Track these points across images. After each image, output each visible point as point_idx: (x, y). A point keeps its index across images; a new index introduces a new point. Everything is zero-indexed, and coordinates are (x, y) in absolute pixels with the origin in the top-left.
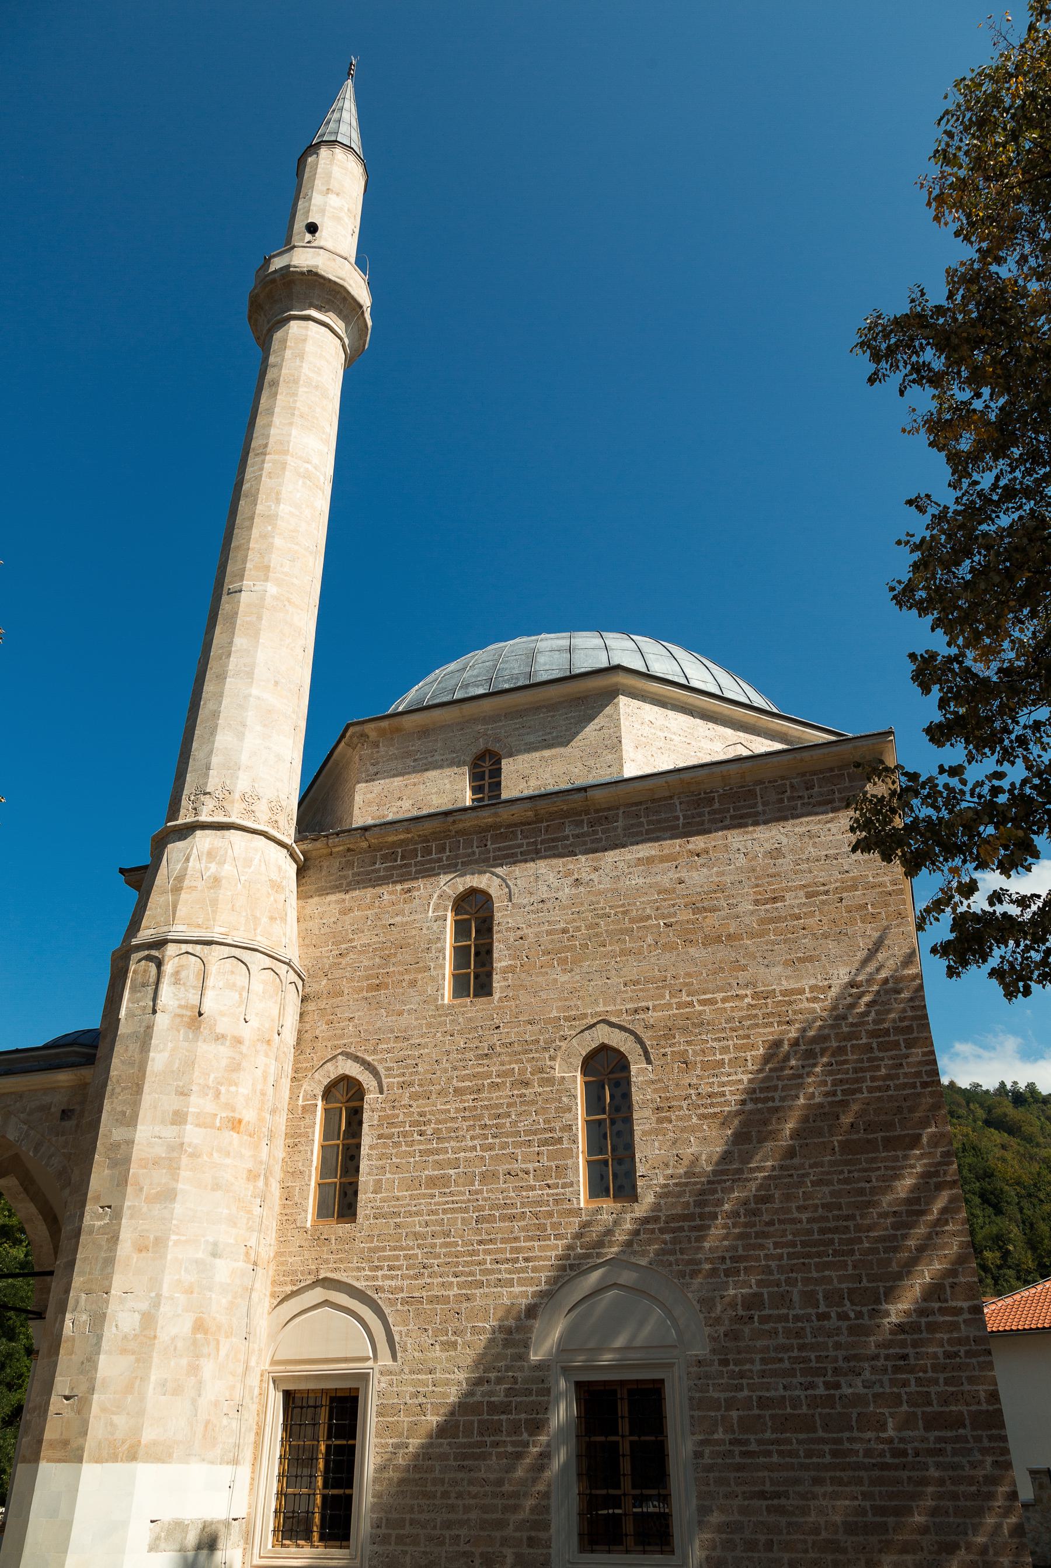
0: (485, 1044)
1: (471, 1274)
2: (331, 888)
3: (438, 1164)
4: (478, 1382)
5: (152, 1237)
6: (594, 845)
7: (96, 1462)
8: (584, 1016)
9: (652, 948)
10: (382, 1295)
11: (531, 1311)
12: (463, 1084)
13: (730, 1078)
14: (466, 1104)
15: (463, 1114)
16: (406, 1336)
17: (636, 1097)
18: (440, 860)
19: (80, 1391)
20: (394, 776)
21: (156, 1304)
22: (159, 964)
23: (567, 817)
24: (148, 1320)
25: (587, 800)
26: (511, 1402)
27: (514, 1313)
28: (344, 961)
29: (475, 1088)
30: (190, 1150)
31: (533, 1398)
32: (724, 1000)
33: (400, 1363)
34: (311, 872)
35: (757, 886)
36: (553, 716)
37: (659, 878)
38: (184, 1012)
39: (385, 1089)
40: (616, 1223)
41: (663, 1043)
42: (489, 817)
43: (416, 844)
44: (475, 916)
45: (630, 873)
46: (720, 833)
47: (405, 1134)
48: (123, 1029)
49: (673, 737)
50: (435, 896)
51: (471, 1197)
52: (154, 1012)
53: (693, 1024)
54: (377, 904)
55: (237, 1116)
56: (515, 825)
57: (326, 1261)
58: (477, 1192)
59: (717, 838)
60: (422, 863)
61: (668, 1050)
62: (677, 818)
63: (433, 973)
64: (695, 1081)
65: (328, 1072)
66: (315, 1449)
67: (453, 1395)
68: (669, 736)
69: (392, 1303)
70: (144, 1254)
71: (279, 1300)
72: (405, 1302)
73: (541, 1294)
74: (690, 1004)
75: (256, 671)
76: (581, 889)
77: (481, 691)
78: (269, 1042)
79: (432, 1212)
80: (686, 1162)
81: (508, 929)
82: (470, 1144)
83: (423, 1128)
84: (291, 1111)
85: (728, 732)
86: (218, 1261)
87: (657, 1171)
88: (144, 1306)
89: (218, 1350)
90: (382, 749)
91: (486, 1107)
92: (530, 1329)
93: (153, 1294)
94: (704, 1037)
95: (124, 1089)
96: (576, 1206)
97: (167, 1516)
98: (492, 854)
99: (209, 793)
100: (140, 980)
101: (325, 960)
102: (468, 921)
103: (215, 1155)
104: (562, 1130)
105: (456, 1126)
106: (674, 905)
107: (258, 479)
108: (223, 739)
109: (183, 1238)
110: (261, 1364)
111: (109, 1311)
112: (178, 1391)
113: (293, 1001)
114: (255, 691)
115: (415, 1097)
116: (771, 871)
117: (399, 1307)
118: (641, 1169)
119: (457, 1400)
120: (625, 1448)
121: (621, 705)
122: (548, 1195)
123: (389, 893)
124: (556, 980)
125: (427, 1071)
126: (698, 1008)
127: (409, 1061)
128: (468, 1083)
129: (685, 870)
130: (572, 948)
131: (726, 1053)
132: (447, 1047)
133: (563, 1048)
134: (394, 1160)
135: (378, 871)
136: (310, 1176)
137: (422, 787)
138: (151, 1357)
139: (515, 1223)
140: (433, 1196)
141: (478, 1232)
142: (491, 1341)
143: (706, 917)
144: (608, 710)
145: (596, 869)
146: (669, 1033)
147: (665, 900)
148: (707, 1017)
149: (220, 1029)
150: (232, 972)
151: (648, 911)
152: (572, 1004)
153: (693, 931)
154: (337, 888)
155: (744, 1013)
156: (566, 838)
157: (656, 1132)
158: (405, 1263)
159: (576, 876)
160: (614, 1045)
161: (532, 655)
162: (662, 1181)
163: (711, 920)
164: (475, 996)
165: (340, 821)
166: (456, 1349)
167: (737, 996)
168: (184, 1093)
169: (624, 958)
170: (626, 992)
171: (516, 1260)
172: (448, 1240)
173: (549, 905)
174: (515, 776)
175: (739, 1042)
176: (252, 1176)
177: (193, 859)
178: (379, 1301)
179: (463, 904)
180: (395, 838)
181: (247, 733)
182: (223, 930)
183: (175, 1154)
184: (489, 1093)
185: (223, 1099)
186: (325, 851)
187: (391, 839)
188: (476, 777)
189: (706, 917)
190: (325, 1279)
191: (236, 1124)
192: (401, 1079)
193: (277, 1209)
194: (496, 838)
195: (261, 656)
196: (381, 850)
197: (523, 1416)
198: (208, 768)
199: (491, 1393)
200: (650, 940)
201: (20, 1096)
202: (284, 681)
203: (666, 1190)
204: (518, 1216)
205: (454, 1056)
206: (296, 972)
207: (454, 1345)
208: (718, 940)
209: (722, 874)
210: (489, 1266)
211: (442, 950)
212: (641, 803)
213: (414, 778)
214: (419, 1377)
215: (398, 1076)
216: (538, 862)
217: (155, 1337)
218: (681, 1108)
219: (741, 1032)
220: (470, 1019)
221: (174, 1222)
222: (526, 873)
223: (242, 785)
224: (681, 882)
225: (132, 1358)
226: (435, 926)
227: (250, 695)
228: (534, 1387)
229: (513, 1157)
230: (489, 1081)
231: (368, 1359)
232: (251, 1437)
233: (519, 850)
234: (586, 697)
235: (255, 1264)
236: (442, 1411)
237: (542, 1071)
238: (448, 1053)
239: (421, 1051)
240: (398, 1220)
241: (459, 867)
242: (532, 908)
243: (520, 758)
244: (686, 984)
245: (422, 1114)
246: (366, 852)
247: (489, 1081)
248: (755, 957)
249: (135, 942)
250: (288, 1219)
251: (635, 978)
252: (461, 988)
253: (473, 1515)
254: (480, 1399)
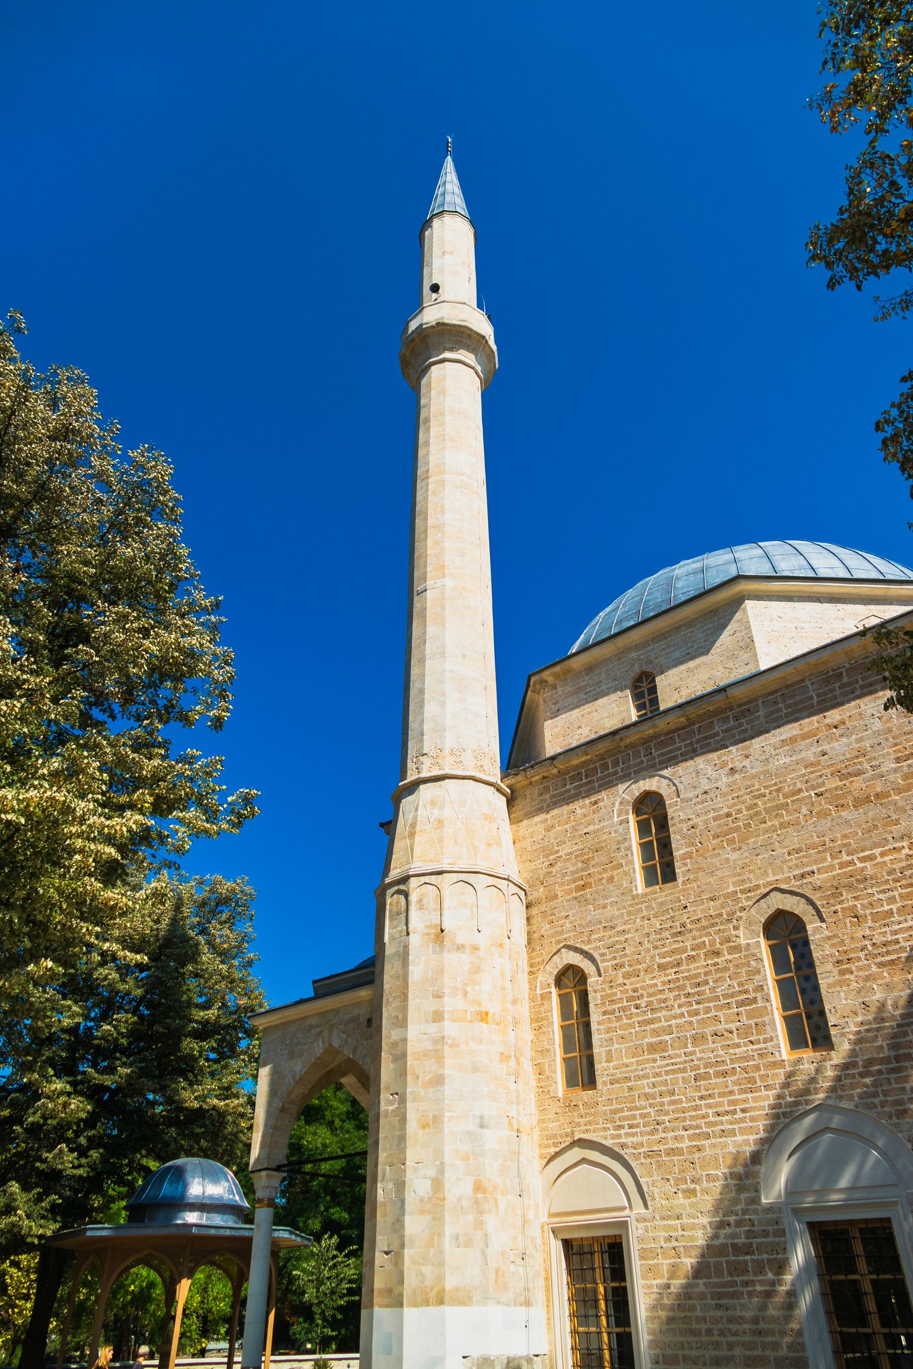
0: (677, 924)
1: (698, 1127)
2: (535, 811)
3: (655, 1032)
4: (721, 1225)
5: (431, 1116)
6: (742, 736)
7: (414, 1306)
8: (758, 887)
9: (808, 817)
10: (627, 1151)
11: (756, 1158)
12: (665, 960)
13: (901, 926)
14: (670, 978)
15: (668, 987)
16: (653, 1186)
17: (816, 954)
18: (616, 773)
19: (395, 1247)
20: (573, 709)
21: (442, 1171)
22: (406, 895)
23: (715, 716)
24: (437, 1184)
25: (728, 698)
26: (751, 1243)
27: (741, 1160)
28: (554, 870)
29: (675, 962)
30: (450, 1041)
31: (771, 1239)
32: (883, 854)
33: (651, 1210)
34: (518, 801)
35: (896, 745)
36: (692, 631)
37: (803, 755)
38: (430, 931)
39: (602, 972)
40: (818, 1071)
41: (832, 901)
42: (649, 729)
43: (596, 762)
44: (652, 812)
45: (777, 754)
46: (853, 703)
47: (624, 1009)
48: (388, 951)
49: (803, 625)
50: (617, 803)
51: (687, 1059)
52: (408, 934)
53: (857, 880)
54: (572, 818)
55: (484, 1009)
56: (672, 731)
57: (579, 1125)
58: (691, 1054)
59: (850, 708)
60: (602, 778)
61: (838, 907)
62: (811, 698)
63: (625, 868)
64: (868, 933)
65: (556, 963)
66: (595, 1291)
67: (700, 1239)
68: (799, 625)
69: (636, 1157)
70: (427, 1130)
71: (546, 1160)
72: (647, 1156)
73: (763, 1142)
74: (851, 863)
76: (737, 776)
77: (632, 623)
78: (501, 945)
79: (657, 1075)
80: (873, 1009)
81: (681, 821)
82: (679, 1011)
83: (638, 1002)
84: (532, 999)
85: (859, 608)
86: (485, 1131)
87: (847, 1020)
88: (432, 1173)
89: (497, 1206)
90: (560, 689)
91: (687, 978)
92: (756, 1175)
93: (438, 1163)
94: (870, 891)
95: (395, 998)
96: (779, 1058)
97: (476, 1353)
98: (657, 761)
100: (395, 910)
101: (540, 871)
102: (648, 820)
103: (471, 1043)
104: (755, 990)
105: (664, 997)
106: (821, 776)
107: (426, 499)
108: (430, 709)
109: (455, 1114)
110: (540, 1217)
111: (407, 1179)
112: (469, 1243)
113: (518, 910)
115: (627, 976)
116: (907, 729)
117: (643, 1160)
118: (832, 1020)
119: (705, 1243)
120: (867, 1287)
121: (748, 608)
122: (752, 1050)
123: (580, 807)
124: (728, 859)
125: (633, 953)
126: (860, 865)
127: (618, 946)
128: (668, 959)
129: (826, 743)
130: (737, 829)
131: (893, 903)
132: (647, 930)
133: (744, 918)
134: (619, 1032)
135: (568, 791)
136: (555, 1053)
137: (595, 714)
138: (443, 1216)
139: (728, 1078)
140: (655, 1060)
141: (698, 1088)
142: (725, 1187)
143: (852, 782)
144: (738, 616)
145: (747, 757)
146: (836, 891)
147: (812, 773)
148: (870, 872)
149: (459, 941)
150: (462, 893)
151: (799, 785)
152: (745, 877)
153: (844, 796)
154: (540, 810)
155: (904, 864)
156: (717, 734)
157: (840, 983)
158: (641, 1121)
159: (731, 766)
160: (789, 909)
161: (670, 583)
162: (854, 1029)
163: (858, 783)
164: (663, 883)
165: (539, 754)
166: (696, 1196)
167: (894, 848)
168: (438, 996)
169: (784, 831)
170: (791, 860)
171: (734, 1112)
172: (673, 1098)
173: (711, 795)
174: (668, 689)
175: (903, 891)
176: (504, 1057)
177: (419, 809)
178: (625, 1156)
179: (641, 806)
180: (578, 761)
182: (450, 861)
183: (439, 1047)
184: (687, 965)
185: (470, 996)
186: (527, 782)
187: (575, 762)
188: (637, 696)
189: (852, 782)
190: (580, 1140)
191: (483, 1016)
192: (614, 962)
193: (533, 1082)
194: (659, 745)
197: (765, 1256)
198: (422, 735)
199: (734, 1236)
200: (804, 811)
201: (337, 1011)
203: (859, 1036)
204: (729, 1072)
205: (653, 936)
206: (516, 885)
207: (693, 1192)
208: (867, 800)
209: (861, 740)
210: (712, 1119)
211: (629, 848)
212: (776, 691)
213: (587, 708)
214: (669, 1222)
215: (611, 960)
216: (696, 759)
217: (444, 1199)
218: (859, 959)
219: (904, 882)
220: (662, 904)
221: (446, 1102)
222: (688, 771)
223: (450, 742)
224: (824, 754)
225: (430, 1217)
226: (621, 829)
228: (770, 1228)
229: (716, 1019)
230: (685, 955)
231: (624, 1208)
232: (541, 1282)
233: (678, 752)
234: (717, 609)
235: (518, 1131)
236: (693, 1254)
237: (728, 940)
238: (648, 935)
239: (626, 937)
240: (630, 1084)
241: (632, 775)
242: (697, 800)
243: (670, 673)
244: (844, 845)
245: (635, 991)
246: (557, 777)
247: (685, 955)
248: (906, 811)
249: (387, 881)
250: (544, 1091)
251: (797, 846)
252: (651, 879)
253: (737, 1352)
254: (725, 1241)
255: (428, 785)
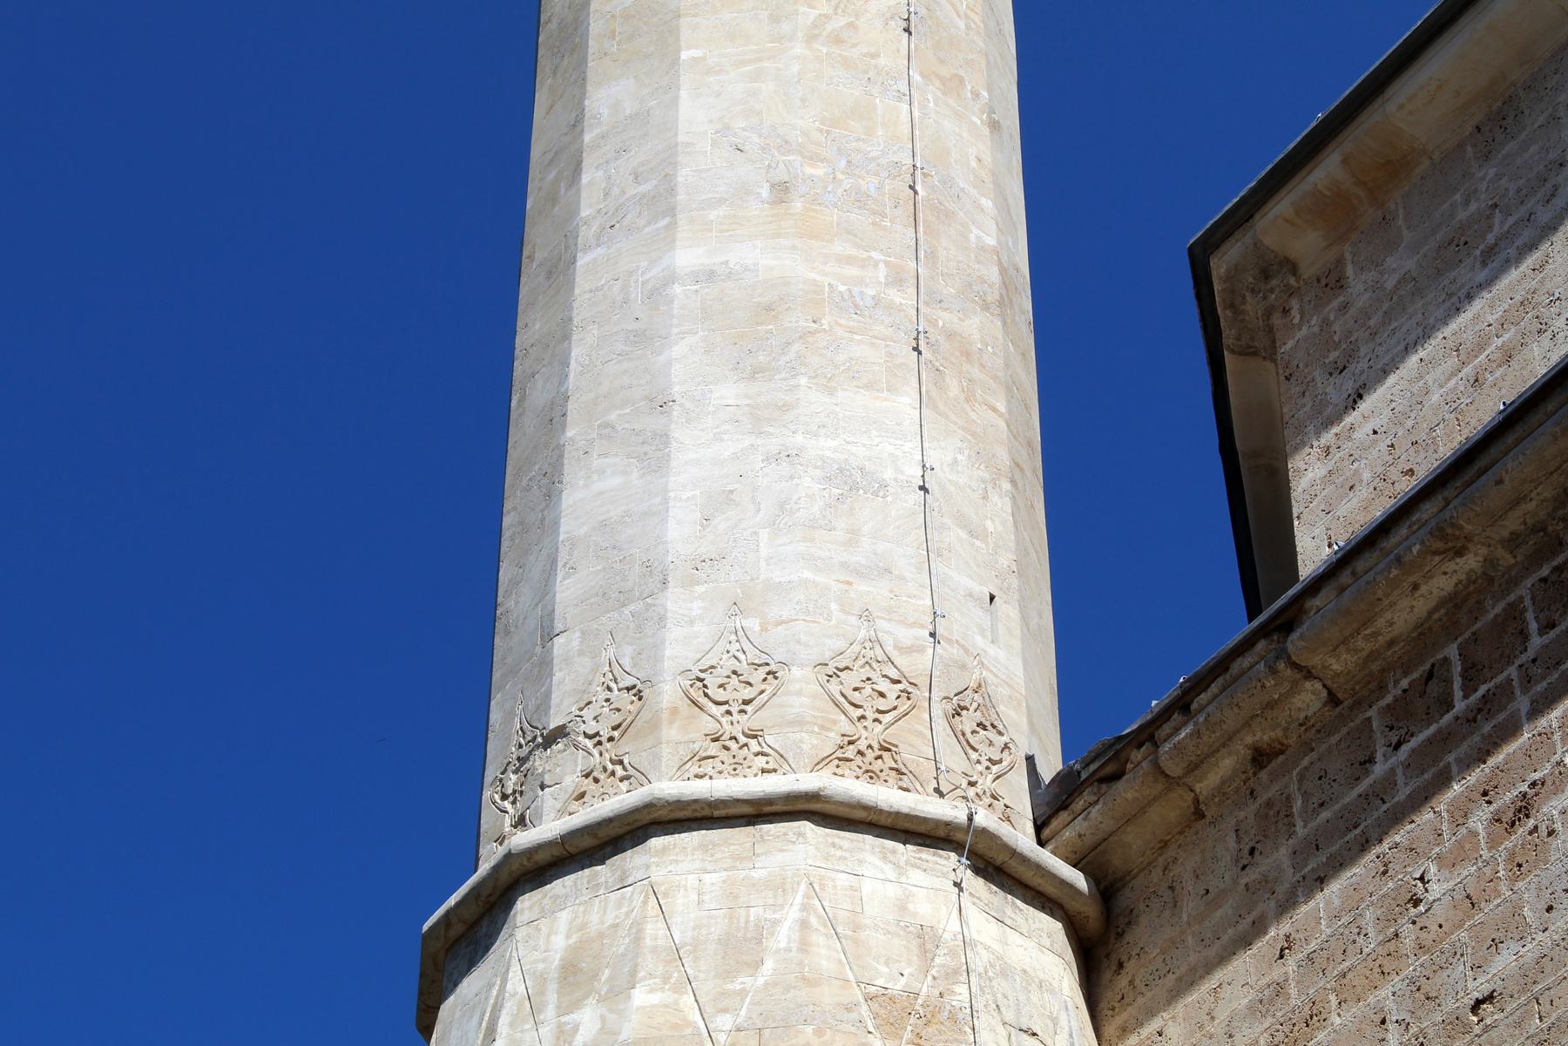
34: (1139, 935)
43: (1514, 583)
54: (1409, 933)
75: (684, 176)
90: (1359, 285)
99: (561, 732)
114: (687, 257)
135: (1389, 781)
181: (679, 433)
186: (1170, 810)
187: (1404, 613)
195: (694, 114)
196: (1382, 689)
198: (549, 636)
202: (819, 171)
227: (670, 279)
255: (561, 886)
